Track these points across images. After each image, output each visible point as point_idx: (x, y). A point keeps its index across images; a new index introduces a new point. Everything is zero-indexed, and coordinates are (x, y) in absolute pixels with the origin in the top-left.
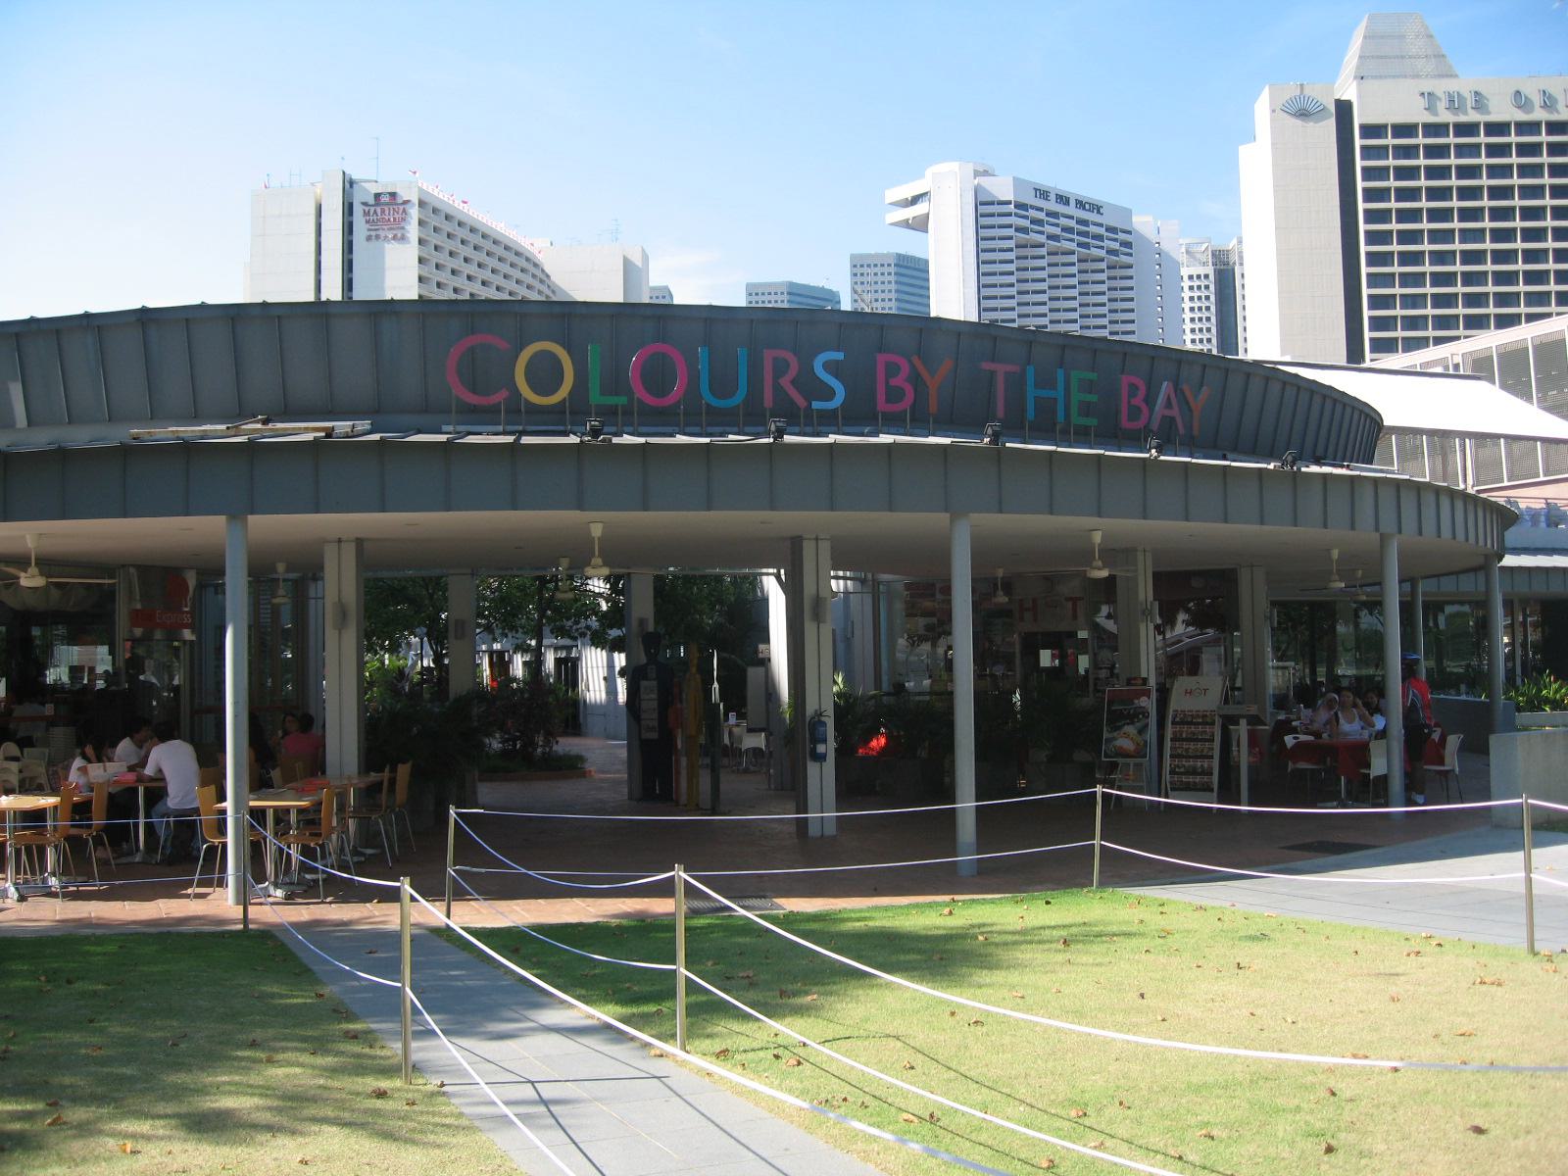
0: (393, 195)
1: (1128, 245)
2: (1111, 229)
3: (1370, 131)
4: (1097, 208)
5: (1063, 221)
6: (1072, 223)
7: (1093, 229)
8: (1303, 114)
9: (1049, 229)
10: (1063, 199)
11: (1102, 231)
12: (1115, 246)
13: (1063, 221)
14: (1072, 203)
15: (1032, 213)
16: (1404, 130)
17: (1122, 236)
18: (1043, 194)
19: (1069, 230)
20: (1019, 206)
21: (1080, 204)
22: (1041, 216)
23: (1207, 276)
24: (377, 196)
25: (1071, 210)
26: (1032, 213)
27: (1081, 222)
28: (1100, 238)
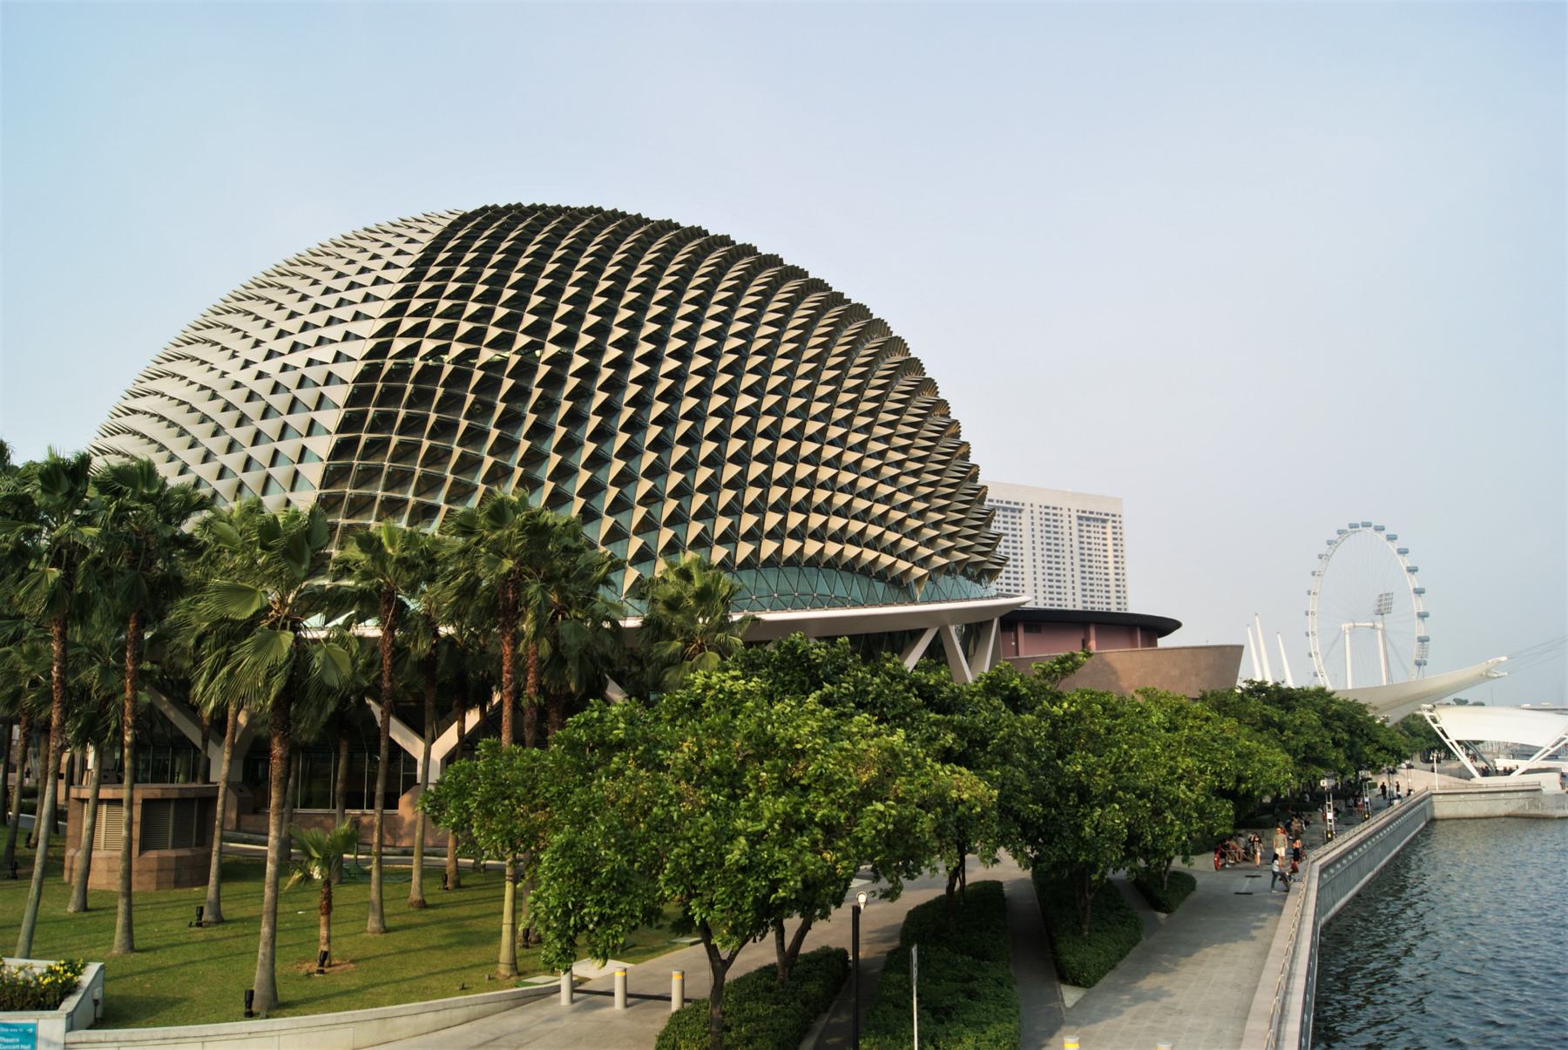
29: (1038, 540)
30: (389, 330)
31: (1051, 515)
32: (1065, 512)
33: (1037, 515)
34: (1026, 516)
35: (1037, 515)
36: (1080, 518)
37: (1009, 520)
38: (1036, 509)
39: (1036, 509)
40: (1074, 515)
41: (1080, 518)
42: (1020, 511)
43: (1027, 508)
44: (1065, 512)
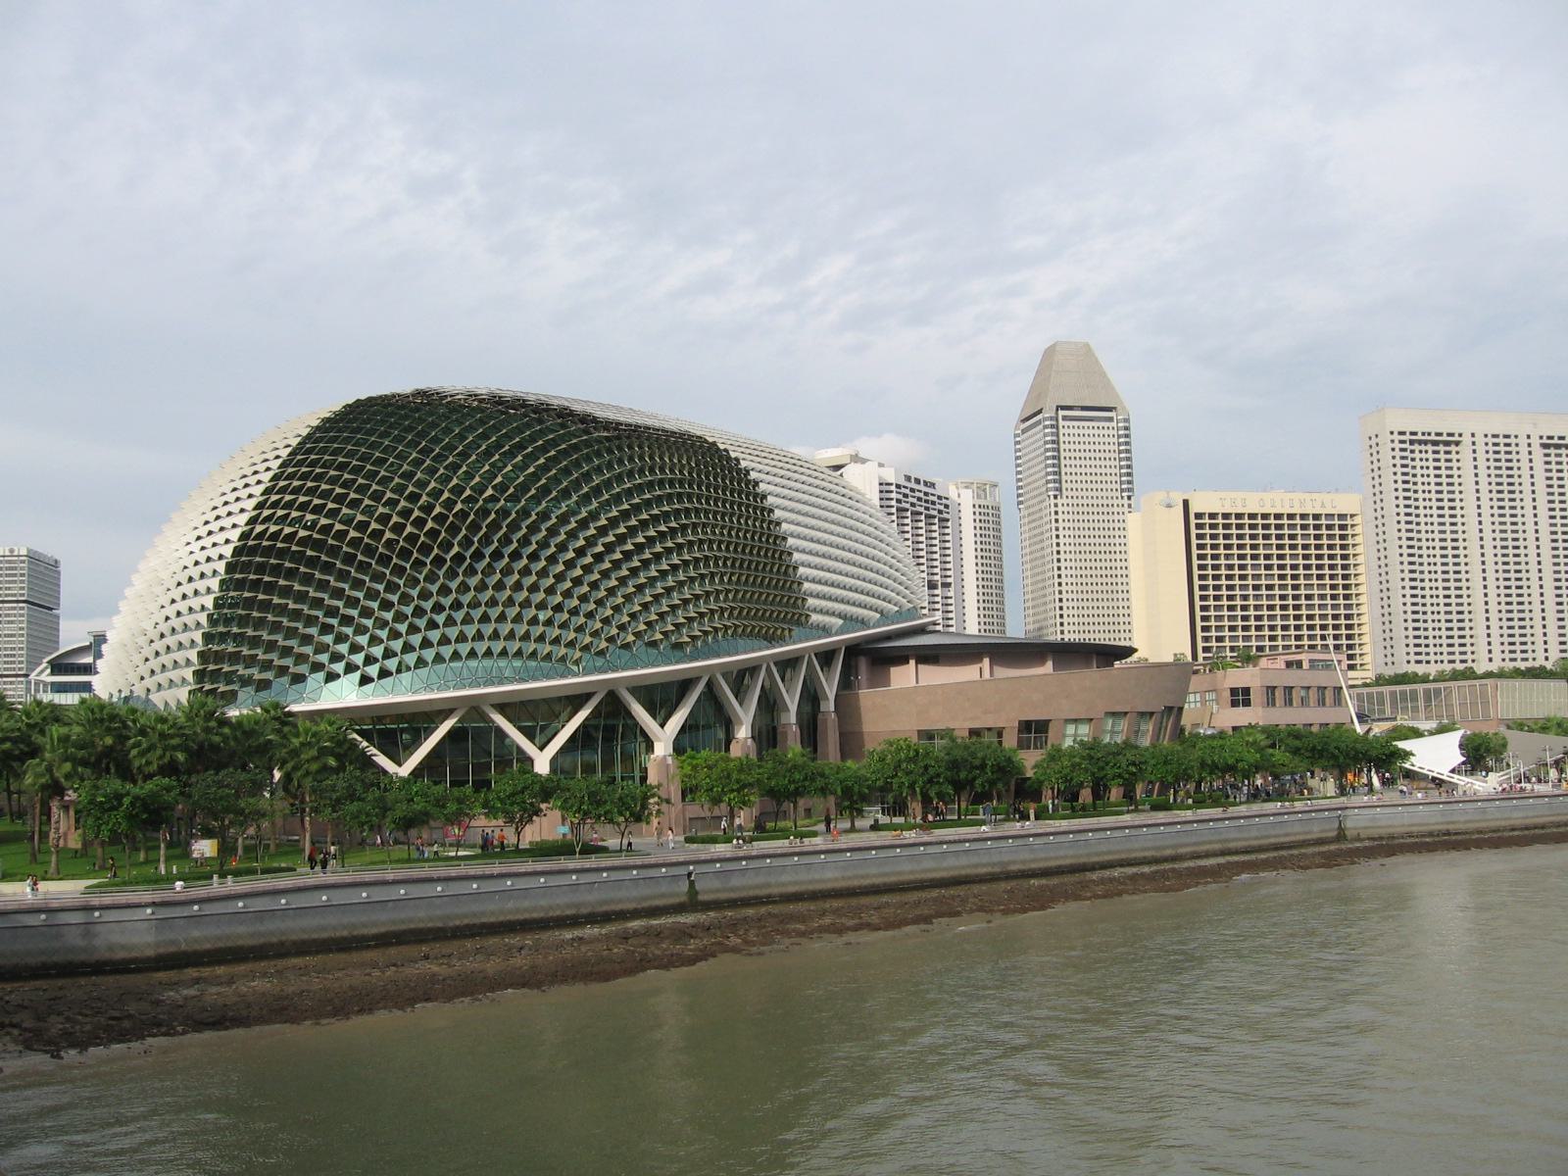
1: (946, 506)
2: (940, 498)
3: (1199, 516)
4: (933, 485)
5: (917, 494)
6: (921, 495)
7: (931, 498)
8: (1169, 506)
9: (911, 500)
10: (918, 481)
11: (935, 499)
12: (942, 508)
13: (917, 494)
15: (903, 490)
16: (1212, 516)
17: (944, 501)
18: (908, 478)
19: (919, 499)
20: (898, 486)
21: (926, 484)
22: (907, 491)
26: (903, 490)
27: (926, 494)
28: (933, 503)
29: (1483, 479)
30: (252, 521)
31: (1502, 447)
32: (1523, 441)
33: (1481, 448)
34: (1466, 449)
35: (1481, 448)
36: (1545, 446)
37: (1442, 456)
38: (1480, 440)
39: (1480, 440)
40: (1536, 442)
41: (1545, 446)
42: (1457, 443)
43: (1467, 440)
44: (1523, 441)
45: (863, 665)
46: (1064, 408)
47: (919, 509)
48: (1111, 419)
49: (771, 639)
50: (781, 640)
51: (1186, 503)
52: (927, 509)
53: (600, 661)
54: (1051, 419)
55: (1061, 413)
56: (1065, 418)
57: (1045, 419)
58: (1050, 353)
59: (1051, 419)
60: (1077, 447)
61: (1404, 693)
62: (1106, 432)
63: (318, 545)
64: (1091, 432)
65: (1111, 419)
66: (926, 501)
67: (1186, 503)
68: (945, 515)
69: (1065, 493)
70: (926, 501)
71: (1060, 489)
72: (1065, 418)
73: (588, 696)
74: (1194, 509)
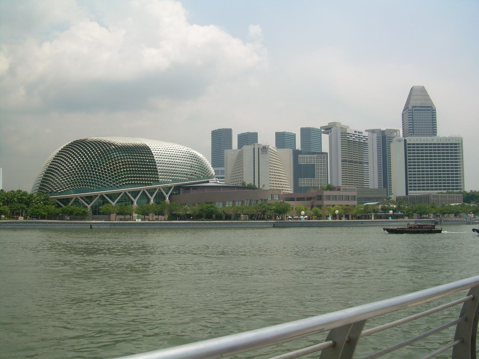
0: (265, 147)
1: (367, 139)
3: (409, 144)
4: (362, 133)
5: (356, 136)
6: (357, 136)
7: (361, 137)
8: (400, 141)
9: (353, 137)
14: (357, 132)
17: (366, 137)
19: (356, 137)
21: (359, 132)
22: (352, 135)
23: (380, 137)
24: (263, 147)
25: (357, 133)
27: (359, 135)
28: (362, 138)
45: (181, 190)
46: (415, 107)
47: (356, 140)
48: (430, 110)
49: (146, 184)
50: (151, 184)
51: (405, 141)
52: (359, 140)
53: (99, 189)
54: (411, 110)
55: (414, 108)
56: (415, 110)
57: (409, 110)
58: (412, 89)
59: (411, 110)
60: (419, 119)
61: (451, 196)
62: (428, 114)
63: (56, 169)
64: (423, 114)
65: (430, 110)
66: (359, 138)
67: (405, 141)
68: (366, 142)
69: (414, 133)
70: (359, 138)
71: (413, 132)
72: (415, 110)
73: (96, 196)
74: (408, 142)
